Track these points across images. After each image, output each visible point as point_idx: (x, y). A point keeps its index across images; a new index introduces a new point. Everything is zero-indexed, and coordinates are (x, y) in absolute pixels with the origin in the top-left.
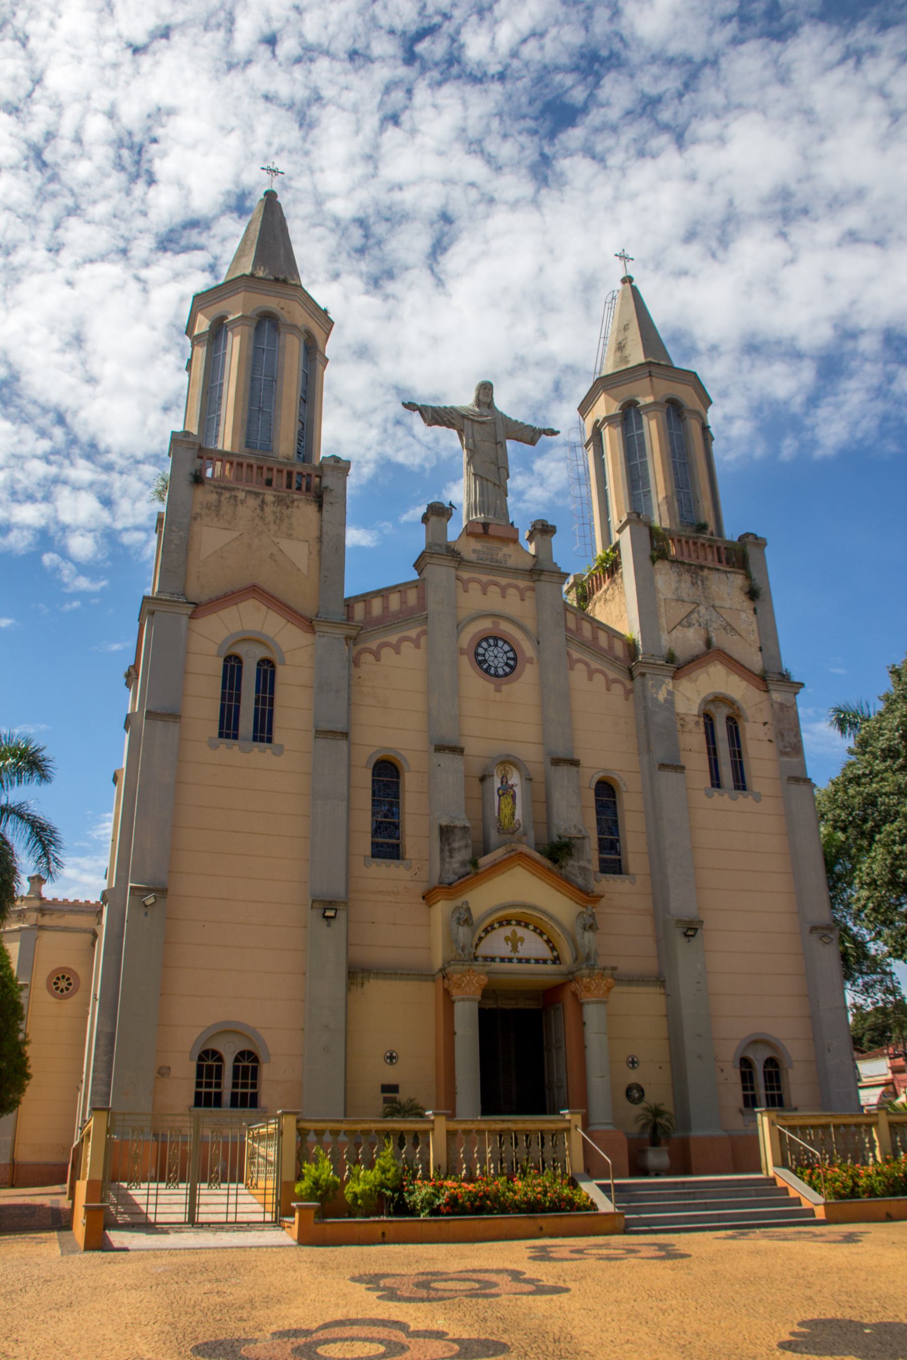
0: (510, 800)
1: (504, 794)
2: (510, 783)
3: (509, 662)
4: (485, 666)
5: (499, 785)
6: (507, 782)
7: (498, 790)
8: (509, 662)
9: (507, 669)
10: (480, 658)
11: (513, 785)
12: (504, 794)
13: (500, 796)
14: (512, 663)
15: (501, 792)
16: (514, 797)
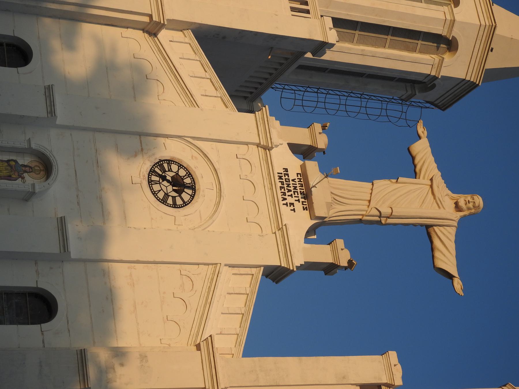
0: (5, 173)
1: (9, 165)
2: (26, 175)
3: (170, 198)
4: (157, 170)
5: (21, 162)
6: (25, 172)
7: (15, 161)
8: (170, 198)
9: (161, 195)
10: (166, 165)
11: (23, 178)
12: (9, 165)
13: (8, 161)
14: (170, 201)
15: (13, 163)
16: (9, 178)
